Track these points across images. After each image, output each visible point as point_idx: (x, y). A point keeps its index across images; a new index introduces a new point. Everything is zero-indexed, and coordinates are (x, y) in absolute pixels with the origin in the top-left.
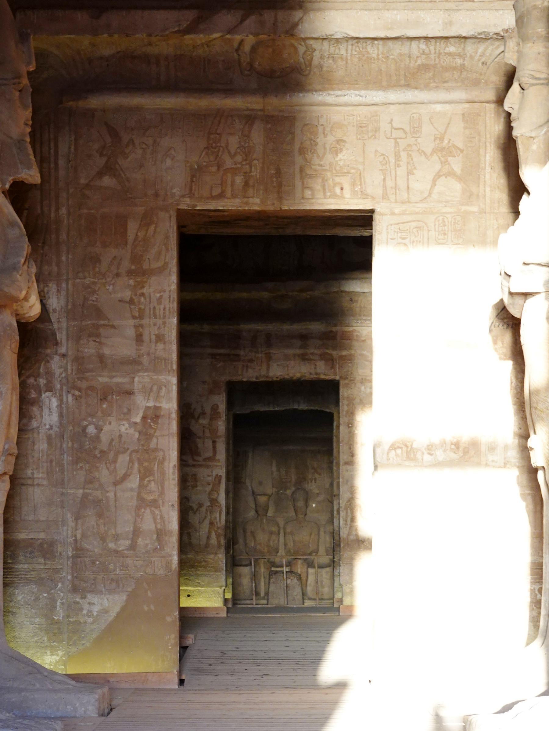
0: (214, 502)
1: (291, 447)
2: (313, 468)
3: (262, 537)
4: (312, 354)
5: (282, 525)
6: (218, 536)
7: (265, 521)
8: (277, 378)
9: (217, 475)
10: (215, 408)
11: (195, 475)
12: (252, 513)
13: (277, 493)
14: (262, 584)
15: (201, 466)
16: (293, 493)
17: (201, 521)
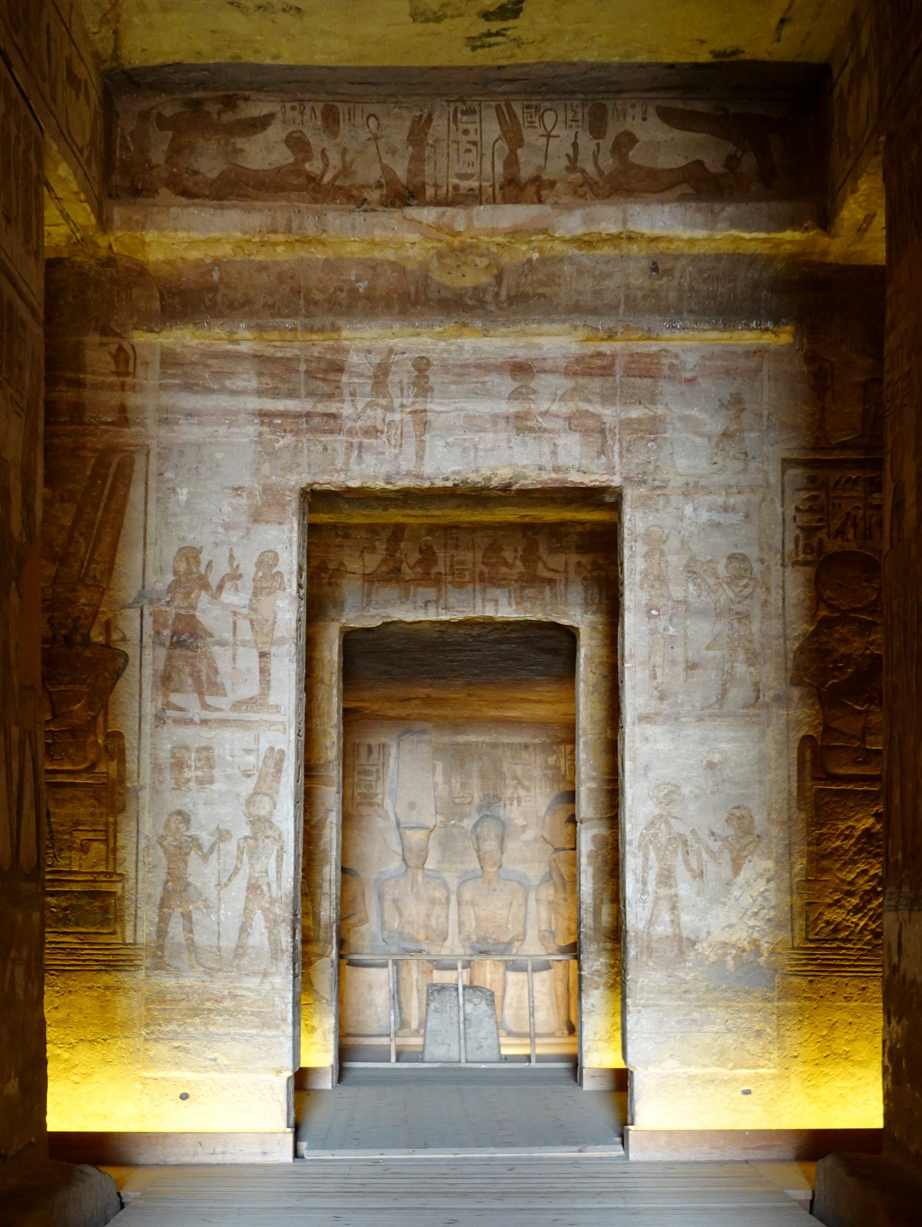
0: (260, 825)
1: (472, 738)
2: (515, 777)
3: (414, 910)
4: (544, 414)
5: (453, 886)
6: (272, 924)
7: (420, 878)
8: (447, 479)
9: (272, 749)
10: (268, 561)
11: (207, 749)
12: (395, 864)
13: (445, 826)
14: (415, 1003)
15: (224, 722)
16: (476, 826)
17: (225, 880)
